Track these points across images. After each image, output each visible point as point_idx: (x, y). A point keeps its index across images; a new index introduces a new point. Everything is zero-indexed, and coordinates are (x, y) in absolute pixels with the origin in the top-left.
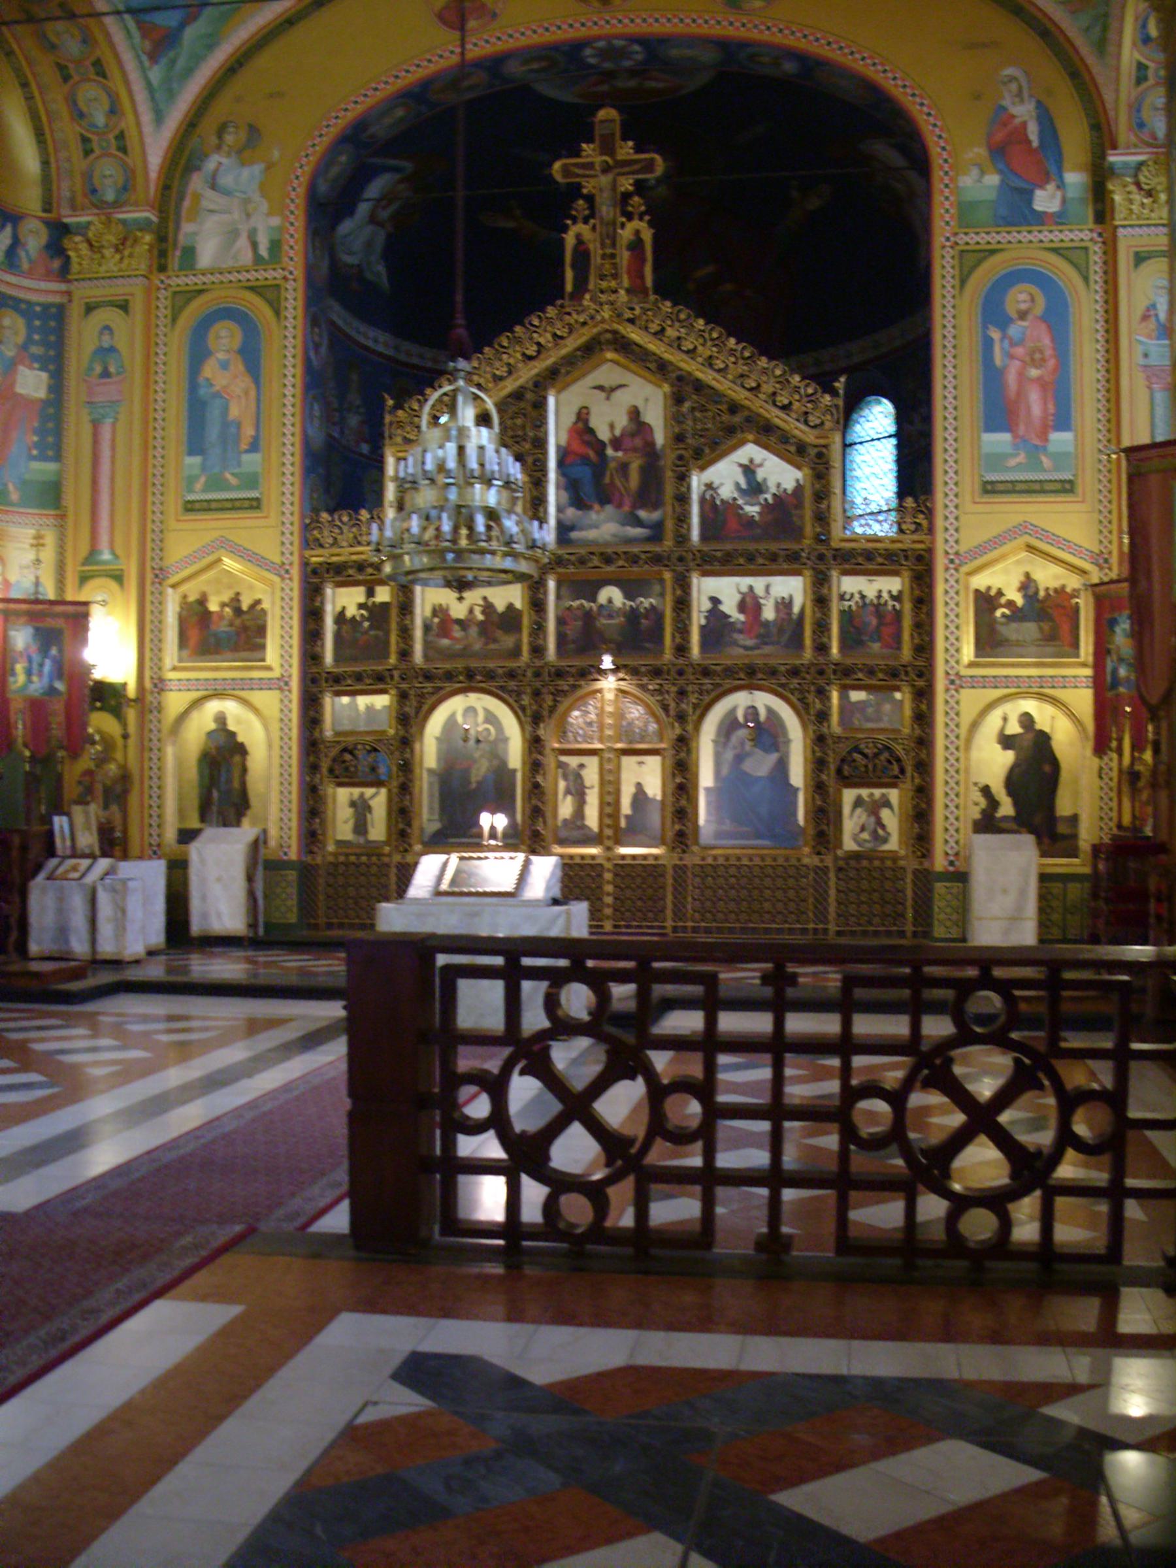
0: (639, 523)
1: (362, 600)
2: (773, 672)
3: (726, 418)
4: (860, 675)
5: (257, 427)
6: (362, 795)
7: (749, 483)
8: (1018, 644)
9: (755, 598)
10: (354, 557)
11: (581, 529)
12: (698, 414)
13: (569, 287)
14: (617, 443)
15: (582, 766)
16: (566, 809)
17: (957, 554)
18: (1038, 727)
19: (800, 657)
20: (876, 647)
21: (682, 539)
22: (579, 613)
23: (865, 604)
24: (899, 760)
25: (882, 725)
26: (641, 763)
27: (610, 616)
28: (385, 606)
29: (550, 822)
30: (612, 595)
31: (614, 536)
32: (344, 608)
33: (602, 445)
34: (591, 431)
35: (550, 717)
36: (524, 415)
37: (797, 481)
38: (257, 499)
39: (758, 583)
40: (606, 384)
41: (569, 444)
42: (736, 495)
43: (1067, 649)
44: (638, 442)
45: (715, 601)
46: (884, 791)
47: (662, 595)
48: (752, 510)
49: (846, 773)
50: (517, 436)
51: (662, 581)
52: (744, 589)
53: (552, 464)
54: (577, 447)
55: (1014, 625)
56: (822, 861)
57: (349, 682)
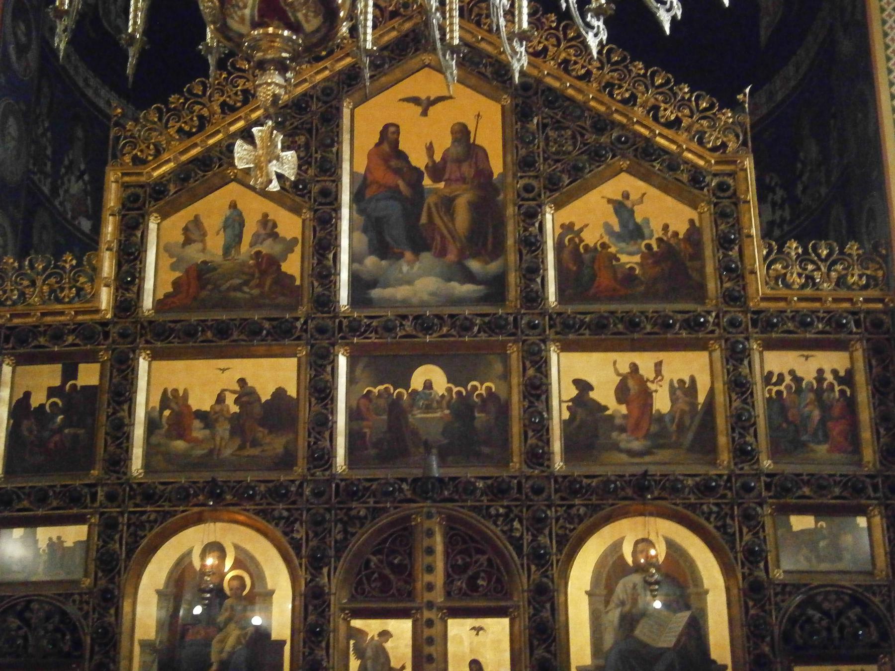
0: (469, 277)
1: (57, 383)
3: (591, 138)
4: (806, 491)
7: (623, 225)
9: (642, 382)
10: (49, 319)
11: (386, 286)
14: (437, 171)
15: (385, 635)
19: (714, 463)
20: (822, 449)
22: (382, 402)
23: (799, 391)
25: (840, 566)
26: (478, 630)
27: (428, 408)
31: (433, 294)
32: (27, 395)
33: (418, 174)
35: (338, 559)
36: (310, 131)
37: (692, 222)
39: (645, 361)
40: (423, 97)
41: (368, 169)
42: (606, 239)
44: (467, 170)
45: (583, 386)
47: (506, 376)
48: (629, 260)
51: (505, 359)
52: (625, 369)
53: (346, 197)
54: (381, 175)
57: (26, 503)
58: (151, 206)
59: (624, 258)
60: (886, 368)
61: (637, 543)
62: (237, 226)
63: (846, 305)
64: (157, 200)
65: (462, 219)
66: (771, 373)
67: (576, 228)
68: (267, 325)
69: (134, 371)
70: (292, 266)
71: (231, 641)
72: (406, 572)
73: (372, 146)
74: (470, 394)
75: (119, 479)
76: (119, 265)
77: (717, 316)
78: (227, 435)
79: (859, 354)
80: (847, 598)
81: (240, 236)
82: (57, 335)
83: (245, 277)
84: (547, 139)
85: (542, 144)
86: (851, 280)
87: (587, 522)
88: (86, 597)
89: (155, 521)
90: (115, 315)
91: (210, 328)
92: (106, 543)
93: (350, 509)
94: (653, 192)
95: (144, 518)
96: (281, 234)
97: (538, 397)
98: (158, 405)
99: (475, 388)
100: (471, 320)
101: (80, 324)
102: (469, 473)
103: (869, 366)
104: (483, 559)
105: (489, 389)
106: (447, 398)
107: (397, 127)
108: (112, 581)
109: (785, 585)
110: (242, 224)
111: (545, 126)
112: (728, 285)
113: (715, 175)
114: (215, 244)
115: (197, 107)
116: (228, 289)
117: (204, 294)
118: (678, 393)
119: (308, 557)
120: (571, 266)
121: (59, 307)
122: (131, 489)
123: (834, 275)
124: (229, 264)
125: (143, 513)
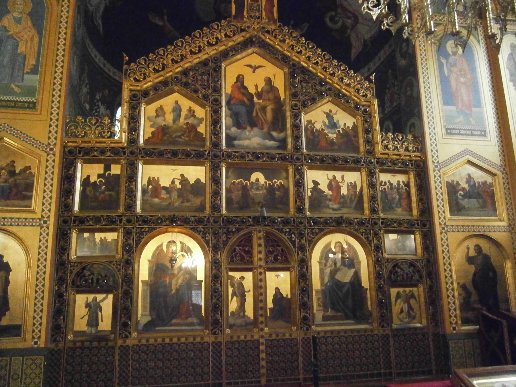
0: (272, 138)
2: (350, 223)
3: (318, 87)
4: (395, 225)
5: (38, 61)
6: (95, 299)
7: (329, 122)
8: (468, 209)
9: (337, 182)
10: (98, 145)
11: (239, 140)
12: (304, 85)
13: (233, 13)
14: (259, 95)
15: (243, 278)
16: (233, 305)
17: (438, 162)
18: (484, 252)
19: (363, 214)
20: (399, 210)
21: (297, 148)
23: (392, 188)
24: (418, 271)
27: (257, 189)
28: (117, 177)
29: (225, 314)
30: (258, 177)
31: (258, 144)
32: (89, 177)
33: (252, 96)
34: (246, 88)
35: (224, 248)
36: (209, 74)
37: (354, 123)
38: (34, 104)
39: (338, 175)
40: (253, 65)
41: (232, 92)
42: (323, 127)
43: (491, 212)
44: (271, 96)
45: (316, 183)
46: (411, 289)
47: (287, 178)
48: (332, 136)
49: (393, 279)
50: (204, 85)
51: (287, 171)
52: (331, 177)
54: (238, 95)
55: (466, 200)
56: (384, 331)
57: (91, 223)
58: (143, 100)
59: (330, 135)
60: (421, 181)
61: (336, 243)
62: (178, 112)
63: (408, 158)
64: (145, 97)
65: (269, 116)
66: (382, 182)
67: (313, 122)
68: (193, 152)
69: (137, 168)
70: (201, 129)
71: (180, 281)
72: (249, 253)
73: (233, 83)
74: (273, 184)
75: (131, 213)
76: (129, 124)
77: (364, 159)
78: (176, 197)
79: (412, 176)
80: (408, 264)
81: (180, 115)
82: (102, 152)
83: (183, 132)
84: (302, 86)
85: (300, 88)
86: (410, 148)
87: (319, 235)
88: (118, 263)
89: (148, 232)
90: (128, 145)
91: (169, 152)
92: (127, 240)
93: (229, 228)
94: (340, 110)
95: (143, 230)
96: (197, 116)
97: (300, 187)
98: (146, 183)
99: (275, 182)
100: (275, 156)
101: (113, 148)
102: (275, 215)
103: (416, 181)
104: (280, 249)
105: (281, 183)
106: (265, 185)
107: (243, 76)
108: (130, 256)
109: (388, 259)
110: (180, 111)
111: (301, 81)
112: (367, 148)
113: (363, 106)
114: (169, 118)
115: (161, 60)
116: (176, 137)
117: (165, 138)
118: (350, 187)
119: (212, 247)
120: (311, 137)
121: (104, 140)
122: (137, 217)
123: (404, 146)
124: (175, 126)
125: (142, 228)
